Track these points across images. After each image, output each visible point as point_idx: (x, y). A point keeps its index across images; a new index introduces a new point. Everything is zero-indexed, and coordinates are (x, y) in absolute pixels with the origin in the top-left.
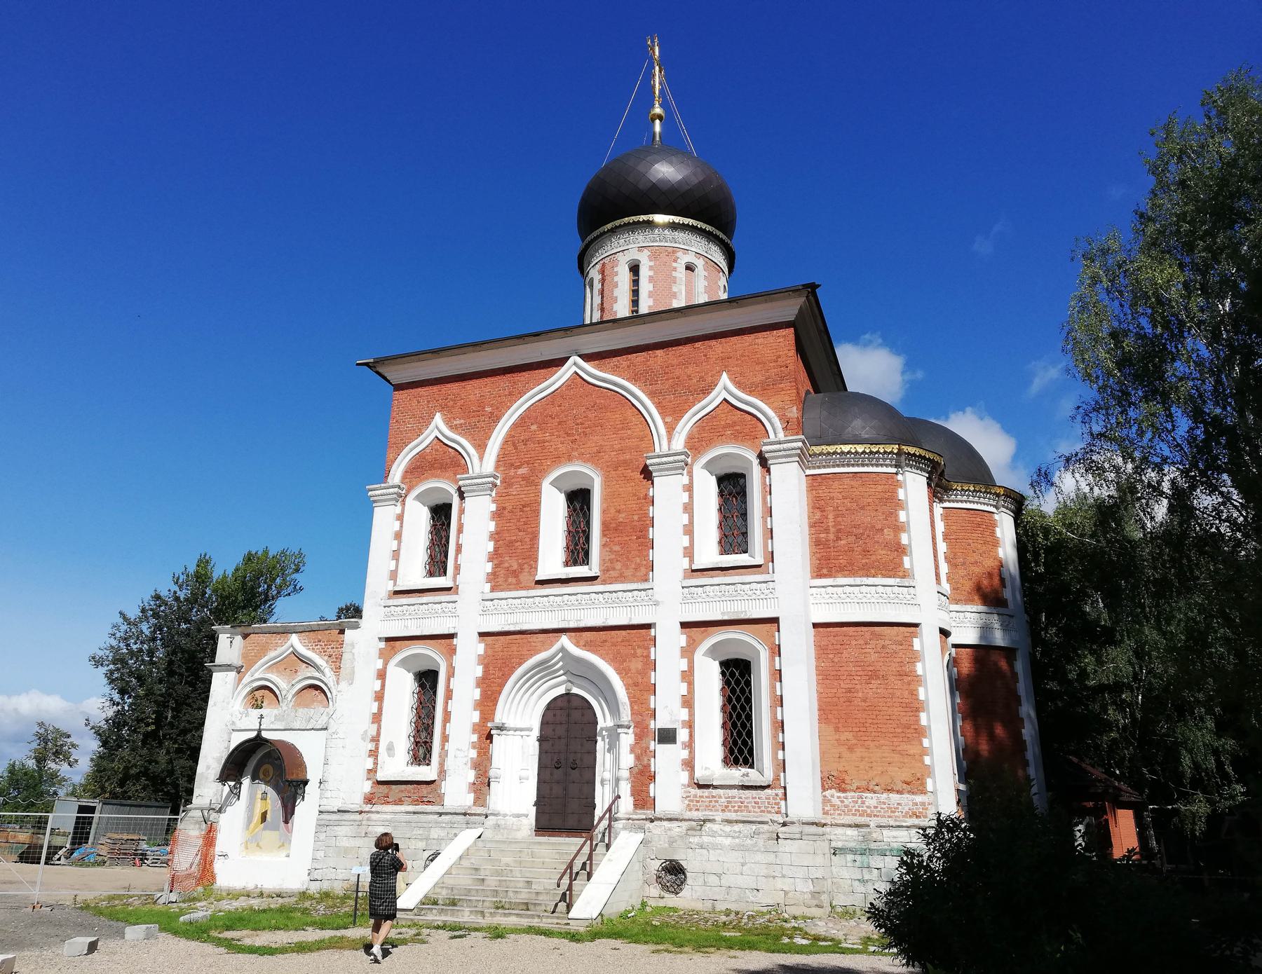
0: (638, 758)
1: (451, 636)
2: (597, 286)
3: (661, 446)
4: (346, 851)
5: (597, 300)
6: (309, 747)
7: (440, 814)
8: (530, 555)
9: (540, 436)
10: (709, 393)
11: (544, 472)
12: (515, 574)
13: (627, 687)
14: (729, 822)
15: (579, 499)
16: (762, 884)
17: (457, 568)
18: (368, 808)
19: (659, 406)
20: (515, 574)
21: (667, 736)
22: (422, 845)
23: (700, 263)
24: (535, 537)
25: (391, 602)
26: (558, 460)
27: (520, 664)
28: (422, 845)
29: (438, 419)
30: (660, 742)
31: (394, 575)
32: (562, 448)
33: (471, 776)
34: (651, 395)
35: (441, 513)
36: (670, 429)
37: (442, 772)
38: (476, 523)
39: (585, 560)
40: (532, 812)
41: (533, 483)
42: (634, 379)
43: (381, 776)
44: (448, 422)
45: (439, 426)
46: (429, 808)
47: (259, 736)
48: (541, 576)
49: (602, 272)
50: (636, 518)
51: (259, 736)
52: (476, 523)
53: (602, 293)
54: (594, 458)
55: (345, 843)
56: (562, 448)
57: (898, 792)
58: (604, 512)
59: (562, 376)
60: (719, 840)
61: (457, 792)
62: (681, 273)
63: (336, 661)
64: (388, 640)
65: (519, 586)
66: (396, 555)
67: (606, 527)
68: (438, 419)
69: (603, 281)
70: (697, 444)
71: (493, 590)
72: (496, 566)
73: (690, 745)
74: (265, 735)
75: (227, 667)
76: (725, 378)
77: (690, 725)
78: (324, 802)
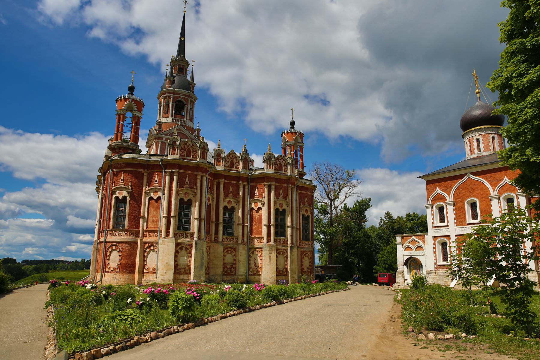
1: (449, 236)
2: (469, 145)
3: (492, 194)
6: (421, 259)
8: (465, 218)
9: (463, 191)
11: (465, 200)
12: (462, 222)
15: (473, 205)
17: (448, 222)
19: (490, 184)
20: (462, 222)
23: (496, 136)
24: (465, 214)
26: (468, 197)
29: (438, 189)
31: (433, 223)
32: (469, 194)
34: (488, 182)
35: (441, 209)
36: (494, 190)
38: (450, 211)
39: (477, 219)
41: (463, 202)
42: (484, 178)
43: (438, 264)
44: (440, 189)
45: (438, 190)
48: (468, 222)
49: (469, 141)
52: (450, 211)
53: (470, 146)
54: (476, 196)
56: (469, 194)
58: (480, 208)
59: (466, 178)
62: (491, 140)
64: (435, 237)
66: (433, 219)
67: (481, 212)
68: (438, 189)
69: (470, 143)
70: (500, 193)
75: (399, 244)
76: (506, 178)
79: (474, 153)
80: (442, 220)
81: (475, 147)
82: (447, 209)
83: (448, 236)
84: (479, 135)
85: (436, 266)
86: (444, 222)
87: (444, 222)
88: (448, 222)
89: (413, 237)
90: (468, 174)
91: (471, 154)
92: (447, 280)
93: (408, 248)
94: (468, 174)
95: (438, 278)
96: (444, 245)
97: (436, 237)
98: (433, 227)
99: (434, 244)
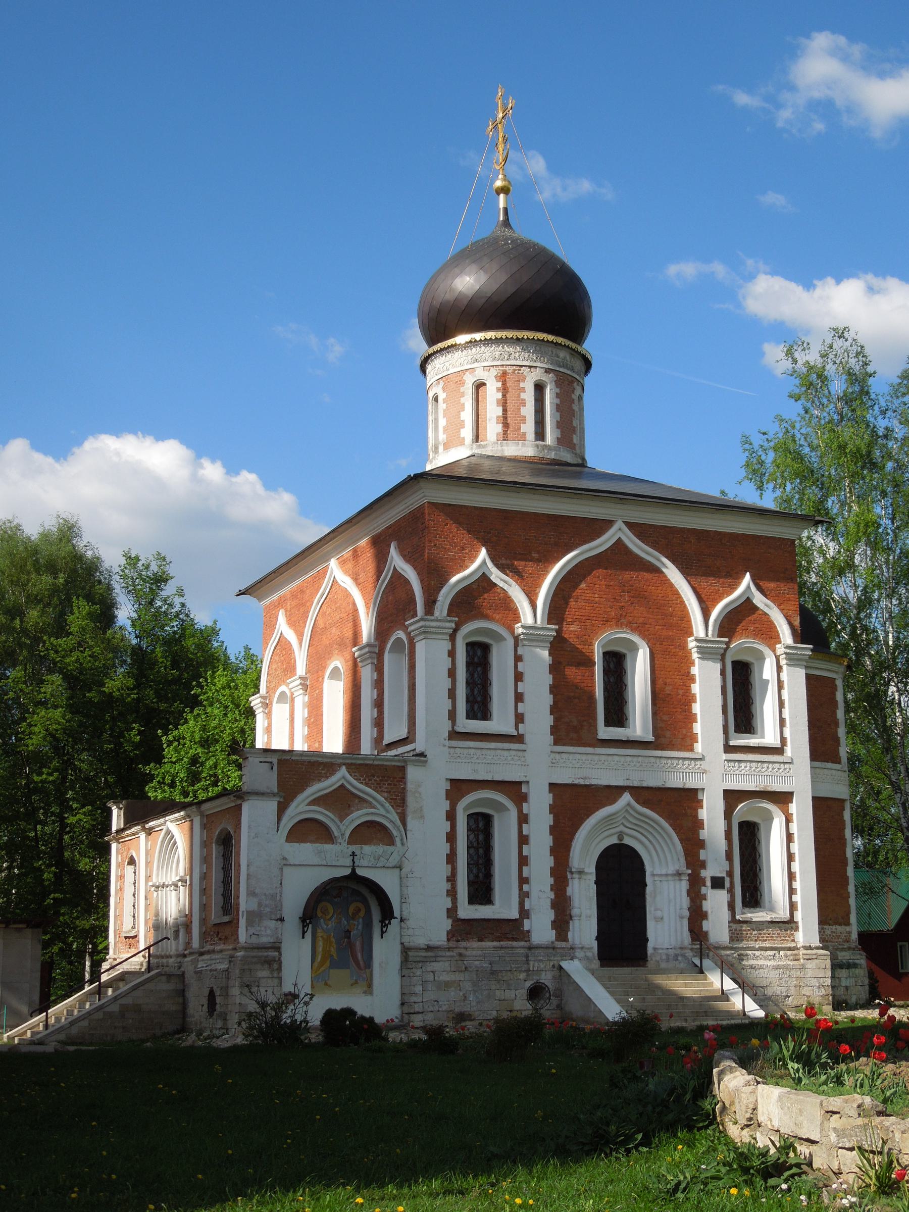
0: (692, 900)
2: (492, 392)
3: (699, 629)
4: (447, 985)
5: (492, 410)
7: (530, 948)
10: (736, 589)
13: (681, 840)
14: (761, 949)
16: (792, 991)
17: (519, 718)
18: (451, 944)
21: (717, 883)
22: (522, 976)
25: (454, 743)
27: (588, 816)
28: (522, 976)
30: (713, 887)
33: (550, 915)
36: (706, 615)
37: (524, 913)
40: (595, 944)
46: (515, 944)
47: (353, 876)
49: (503, 377)
50: (681, 692)
51: (353, 876)
55: (445, 977)
57: (840, 925)
60: (761, 962)
61: (541, 928)
63: (399, 800)
64: (452, 781)
65: (580, 743)
69: (505, 390)
71: (556, 743)
72: (556, 720)
73: (731, 891)
74: (360, 872)
77: (730, 874)
78: (406, 940)
79: (523, 437)
80: (479, 705)
81: (528, 411)
82: (518, 658)
83: (515, 791)
84: (547, 371)
85: (447, 924)
86: (485, 715)
87: (485, 715)
88: (519, 718)
89: (343, 771)
90: (619, 524)
91: (505, 436)
92: (510, 994)
93: (308, 830)
94: (619, 524)
95: (468, 986)
96: (481, 826)
97: (458, 788)
98: (455, 735)
99: (451, 816)
